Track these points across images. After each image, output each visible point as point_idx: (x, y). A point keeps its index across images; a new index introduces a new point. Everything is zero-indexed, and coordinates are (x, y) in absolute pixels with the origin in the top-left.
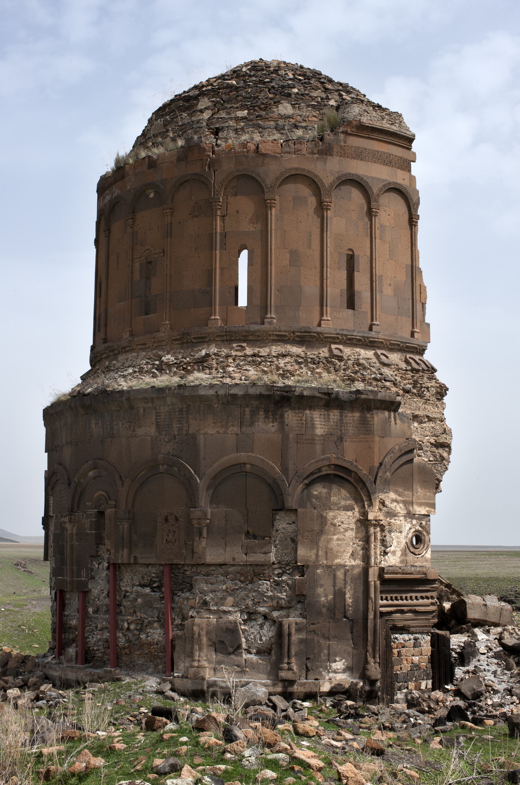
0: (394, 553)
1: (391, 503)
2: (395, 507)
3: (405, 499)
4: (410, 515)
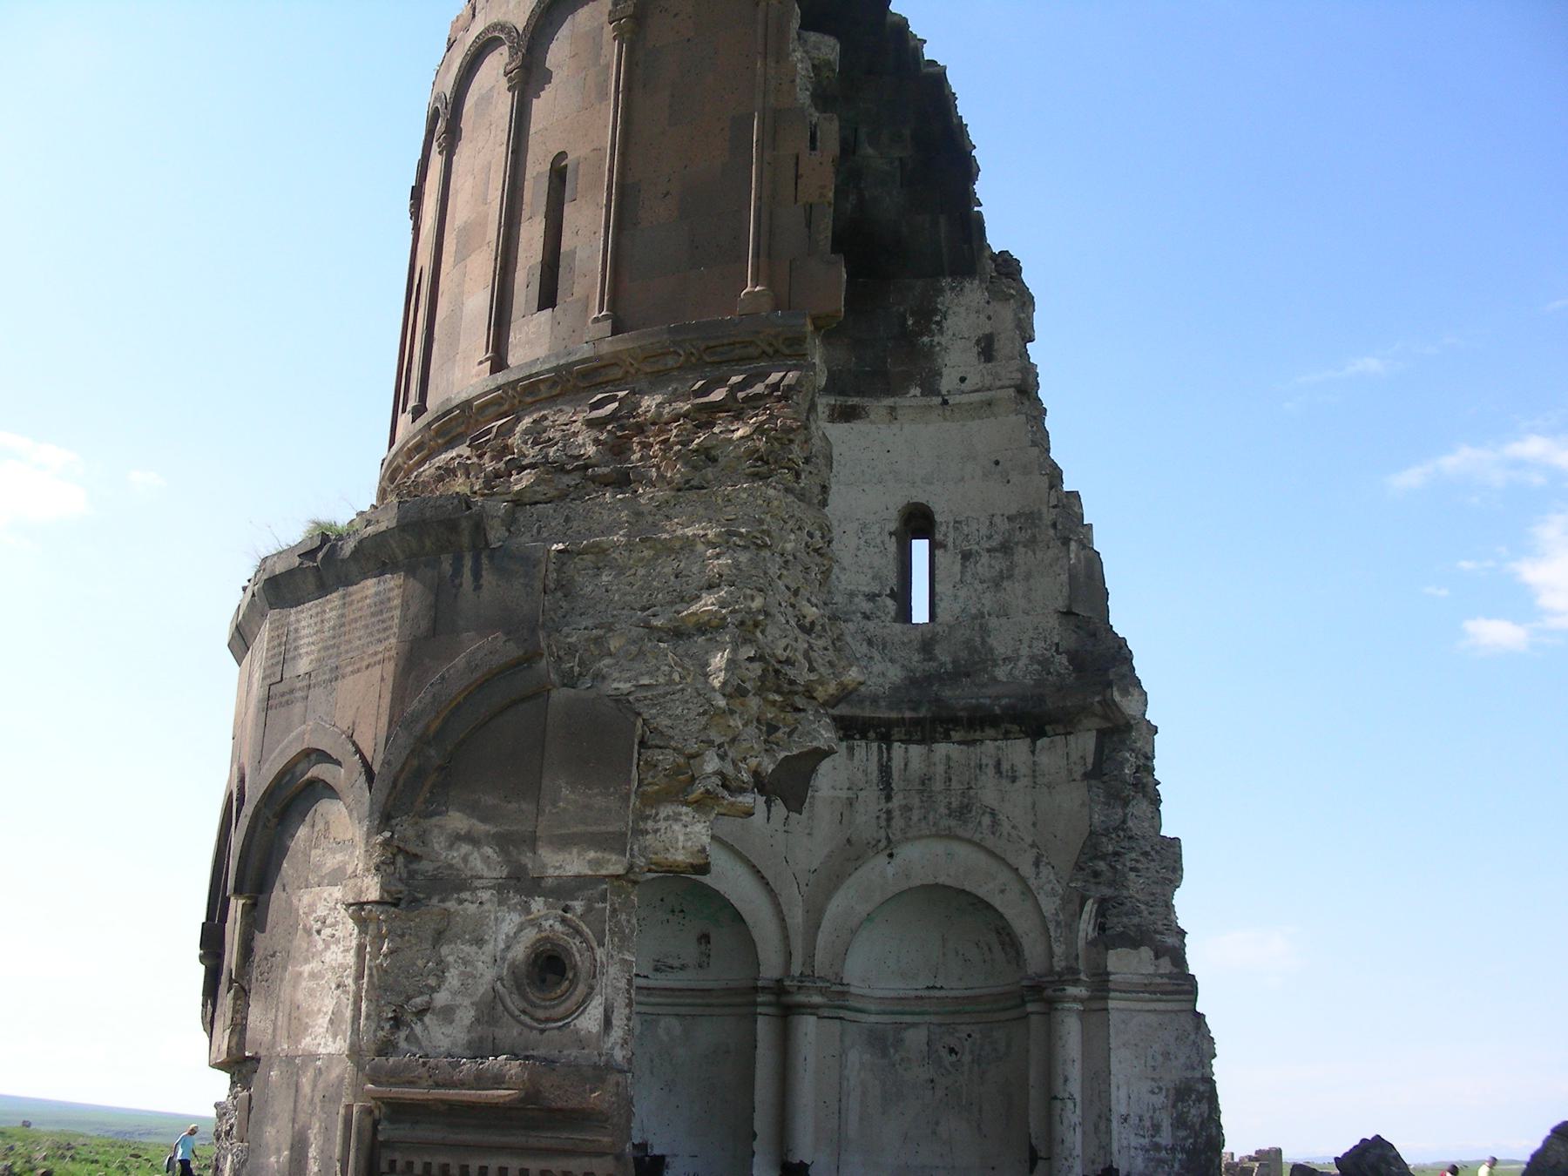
0: (447, 1013)
1: (451, 847)
2: (465, 859)
4: (521, 883)
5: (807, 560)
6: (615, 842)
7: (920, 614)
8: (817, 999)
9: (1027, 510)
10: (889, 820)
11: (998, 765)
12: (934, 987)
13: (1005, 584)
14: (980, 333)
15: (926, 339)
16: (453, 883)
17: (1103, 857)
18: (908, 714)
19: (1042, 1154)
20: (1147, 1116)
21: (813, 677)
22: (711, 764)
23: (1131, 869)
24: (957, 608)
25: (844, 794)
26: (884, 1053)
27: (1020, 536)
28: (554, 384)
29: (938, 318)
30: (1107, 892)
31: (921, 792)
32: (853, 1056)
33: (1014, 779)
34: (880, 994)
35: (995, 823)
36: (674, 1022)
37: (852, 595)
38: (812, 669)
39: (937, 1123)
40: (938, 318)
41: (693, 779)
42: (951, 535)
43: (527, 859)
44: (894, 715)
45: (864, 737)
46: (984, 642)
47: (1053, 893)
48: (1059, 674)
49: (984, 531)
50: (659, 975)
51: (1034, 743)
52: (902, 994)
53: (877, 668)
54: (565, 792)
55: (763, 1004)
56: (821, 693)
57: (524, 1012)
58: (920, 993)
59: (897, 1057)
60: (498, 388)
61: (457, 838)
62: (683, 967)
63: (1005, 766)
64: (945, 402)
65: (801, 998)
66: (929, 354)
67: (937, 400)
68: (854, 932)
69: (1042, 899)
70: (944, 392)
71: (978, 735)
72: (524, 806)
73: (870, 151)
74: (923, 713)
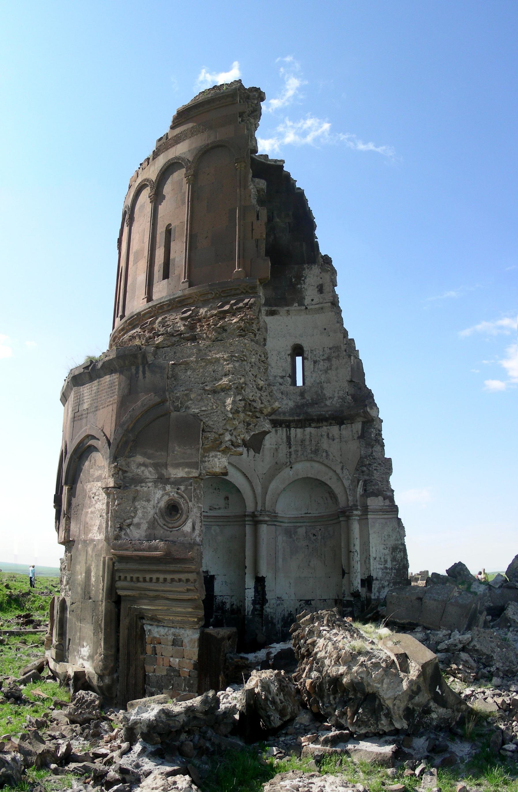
0: (138, 526)
1: (138, 468)
2: (143, 472)
3: (156, 461)
4: (162, 480)
5: (259, 365)
6: (195, 465)
7: (299, 382)
8: (267, 518)
9: (336, 345)
10: (290, 455)
11: (328, 435)
12: (307, 513)
13: (329, 371)
14: (318, 284)
15: (299, 286)
16: (139, 481)
17: (365, 466)
18: (296, 418)
19: (346, 572)
20: (382, 557)
21: (262, 406)
22: (228, 437)
23: (375, 470)
24: (312, 380)
25: (274, 447)
26: (291, 537)
27: (333, 355)
28: (169, 305)
29: (303, 279)
30: (367, 478)
31: (301, 445)
32: (280, 538)
33: (333, 440)
34: (288, 516)
35: (327, 455)
36: (217, 528)
37: (275, 377)
38: (262, 403)
39: (310, 562)
40: (303, 279)
41: (221, 442)
42: (310, 355)
43: (164, 472)
44: (291, 418)
45: (281, 426)
46: (322, 392)
47: (348, 479)
48: (348, 403)
49: (321, 353)
50: (211, 511)
51: (340, 427)
52: (296, 516)
53: (285, 402)
54: (177, 448)
55: (248, 521)
56: (265, 411)
57: (164, 525)
58: (302, 515)
59: (295, 538)
60: (150, 308)
61: (140, 465)
62: (219, 508)
63: (330, 435)
64: (306, 308)
65: (261, 518)
66: (300, 291)
67: (304, 308)
68: (279, 495)
69: (344, 481)
70: (306, 305)
71: (321, 425)
72: (163, 453)
73: (278, 220)
74: (301, 417)
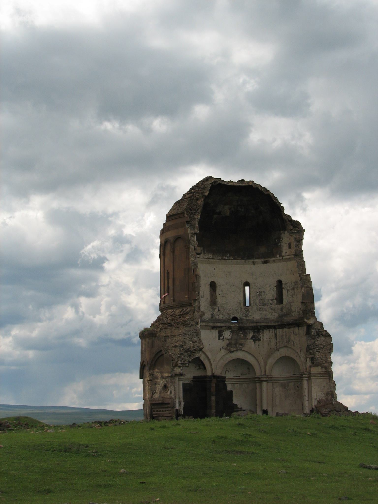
4: (162, 377)
17: (311, 349)
18: (277, 324)
30: (312, 356)
33: (296, 335)
35: (294, 344)
37: (268, 300)
53: (273, 314)
65: (262, 379)
74: (279, 323)
